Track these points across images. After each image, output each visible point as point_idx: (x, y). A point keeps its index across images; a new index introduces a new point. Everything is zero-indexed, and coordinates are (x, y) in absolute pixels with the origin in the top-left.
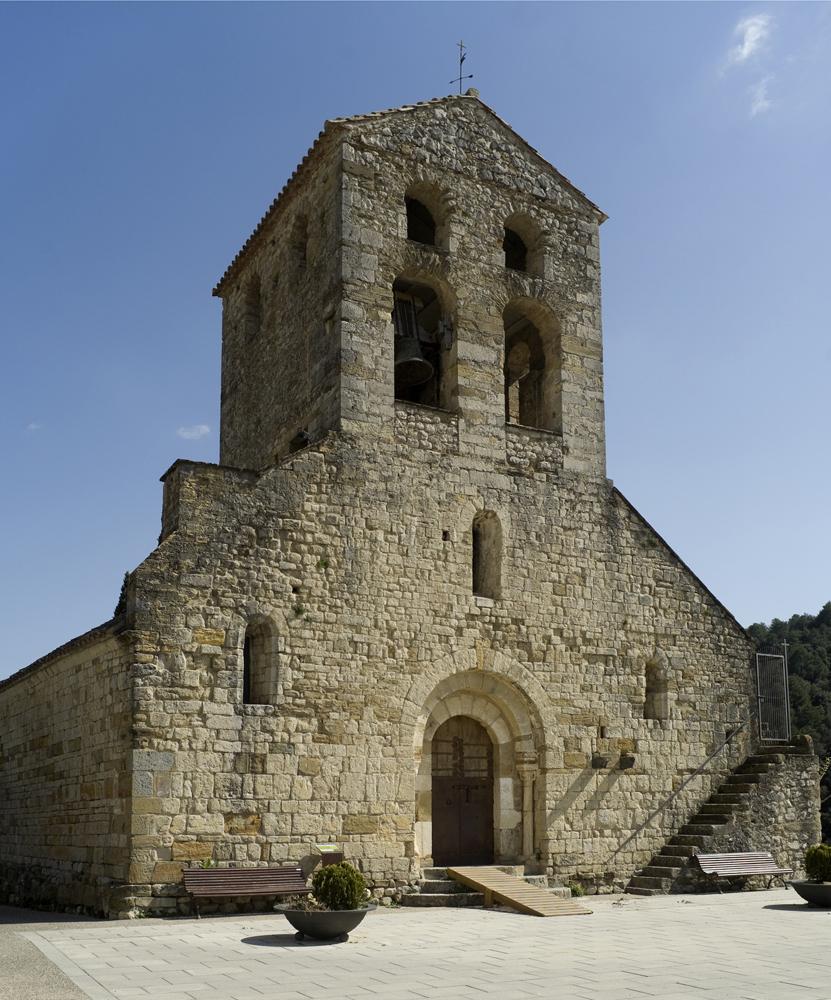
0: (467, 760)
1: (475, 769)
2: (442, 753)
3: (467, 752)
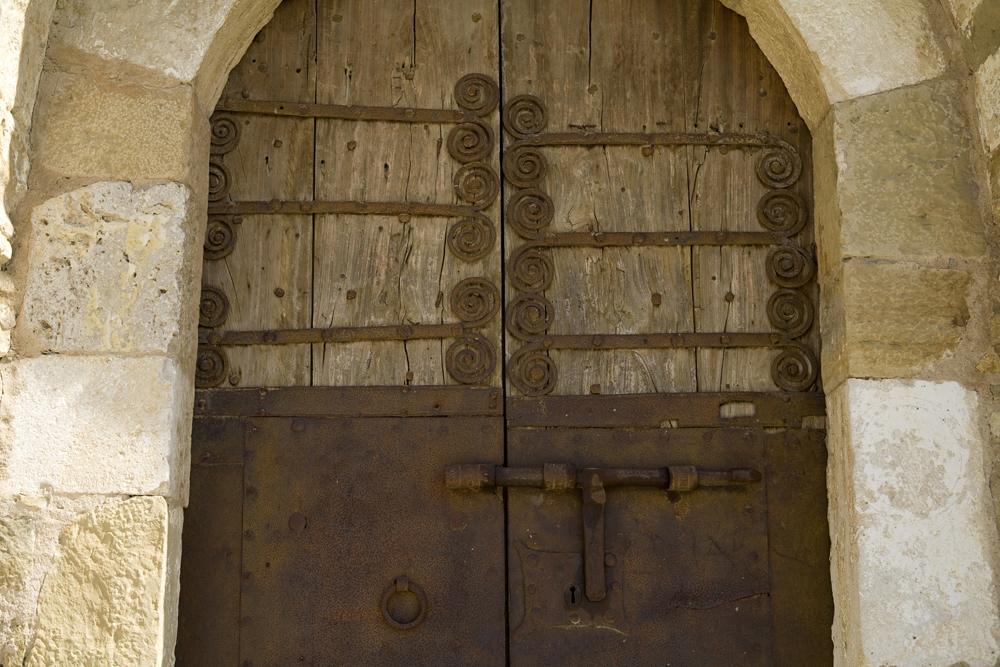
0: (588, 261)
1: (648, 325)
2: (361, 208)
3: (578, 196)
